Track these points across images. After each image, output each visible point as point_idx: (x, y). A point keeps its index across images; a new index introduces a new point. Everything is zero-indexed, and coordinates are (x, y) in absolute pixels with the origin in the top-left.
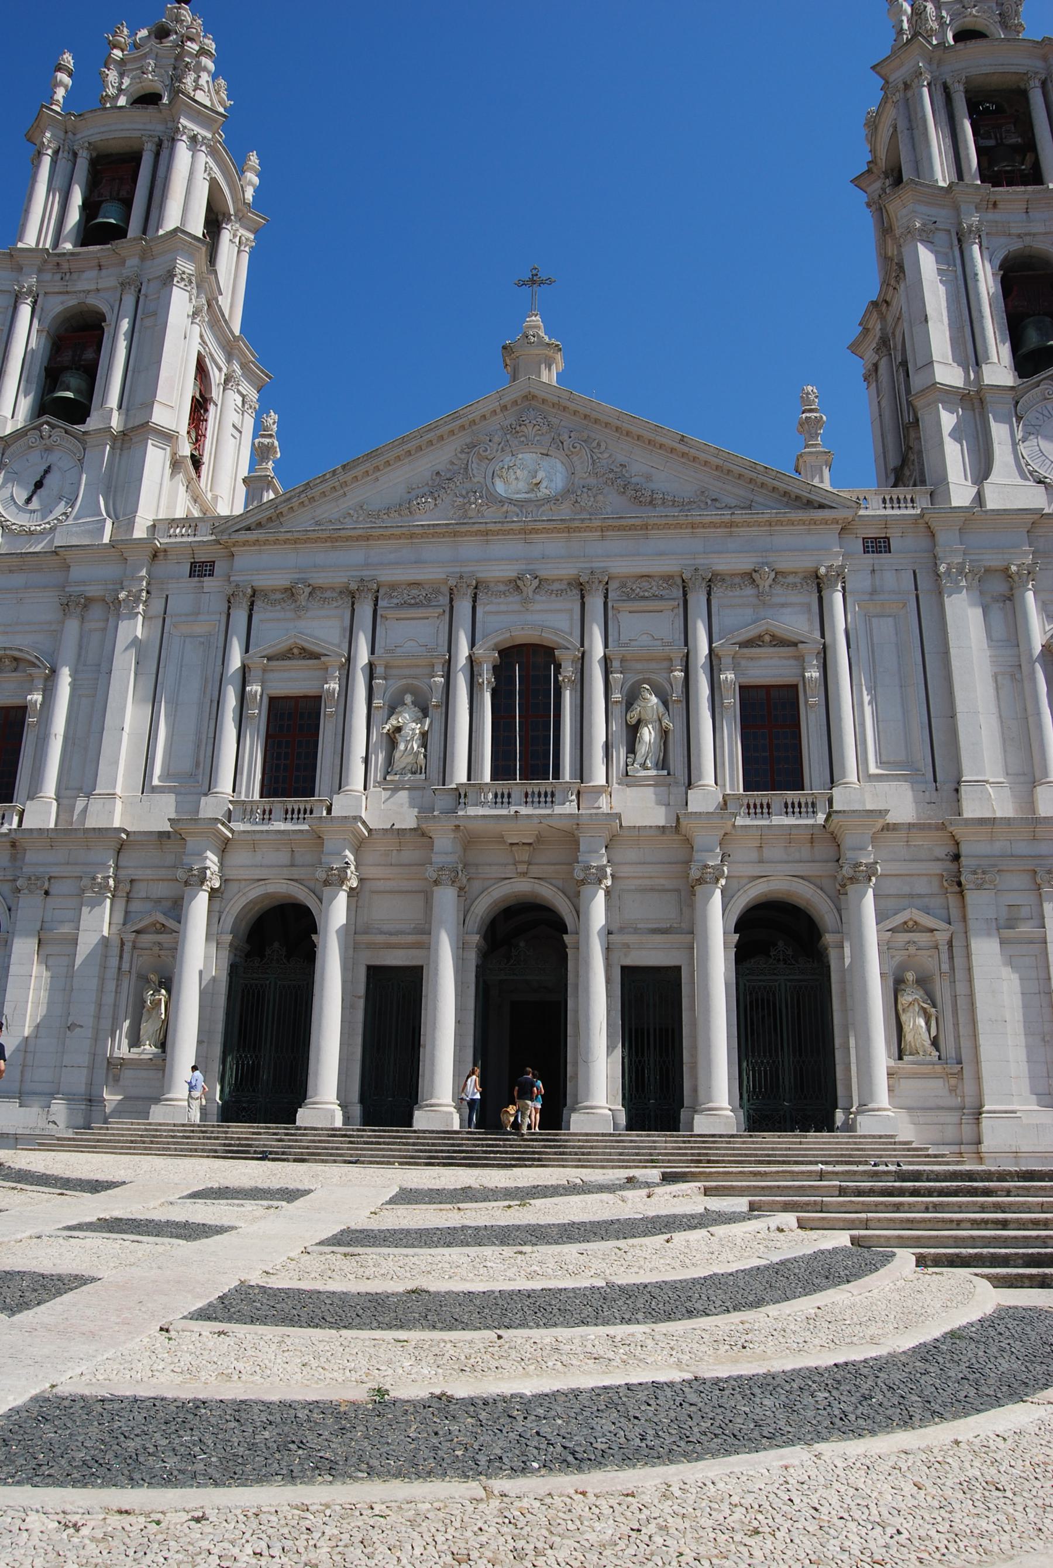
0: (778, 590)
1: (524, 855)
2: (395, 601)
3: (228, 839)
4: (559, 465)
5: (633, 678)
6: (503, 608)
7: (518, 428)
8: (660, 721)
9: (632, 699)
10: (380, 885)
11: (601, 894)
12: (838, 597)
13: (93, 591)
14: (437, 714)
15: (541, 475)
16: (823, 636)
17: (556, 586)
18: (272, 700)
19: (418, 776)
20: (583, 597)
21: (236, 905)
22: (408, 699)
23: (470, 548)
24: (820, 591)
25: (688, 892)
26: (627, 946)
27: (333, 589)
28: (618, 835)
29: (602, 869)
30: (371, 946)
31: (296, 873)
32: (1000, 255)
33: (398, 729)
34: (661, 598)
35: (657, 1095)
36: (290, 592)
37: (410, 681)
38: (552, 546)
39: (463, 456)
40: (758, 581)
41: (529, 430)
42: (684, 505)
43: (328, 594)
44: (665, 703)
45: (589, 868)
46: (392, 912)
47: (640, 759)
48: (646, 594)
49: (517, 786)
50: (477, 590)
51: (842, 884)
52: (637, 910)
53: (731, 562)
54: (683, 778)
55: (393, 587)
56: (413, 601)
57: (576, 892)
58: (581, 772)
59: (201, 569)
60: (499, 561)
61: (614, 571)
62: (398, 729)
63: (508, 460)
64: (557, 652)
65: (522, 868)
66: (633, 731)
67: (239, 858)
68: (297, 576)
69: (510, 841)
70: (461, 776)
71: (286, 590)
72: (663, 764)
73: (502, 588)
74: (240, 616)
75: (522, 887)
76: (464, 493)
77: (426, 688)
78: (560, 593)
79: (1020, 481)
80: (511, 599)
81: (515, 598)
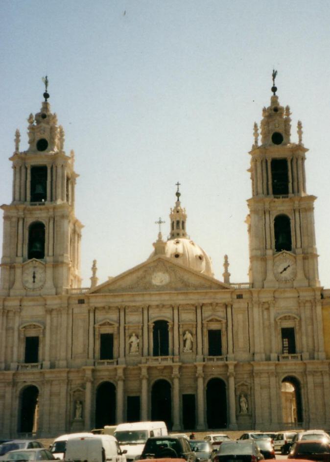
0: (217, 308)
4: (168, 277)
9: (184, 334)
13: (55, 307)
15: (163, 279)
22: (134, 335)
25: (196, 379)
33: (132, 342)
38: (166, 297)
42: (196, 288)
44: (192, 334)
46: (133, 385)
47: (186, 349)
53: (206, 301)
54: (195, 353)
55: (129, 307)
59: (81, 302)
60: (155, 300)
62: (132, 342)
66: (185, 341)
72: (191, 349)
74: (92, 315)
78: (168, 308)
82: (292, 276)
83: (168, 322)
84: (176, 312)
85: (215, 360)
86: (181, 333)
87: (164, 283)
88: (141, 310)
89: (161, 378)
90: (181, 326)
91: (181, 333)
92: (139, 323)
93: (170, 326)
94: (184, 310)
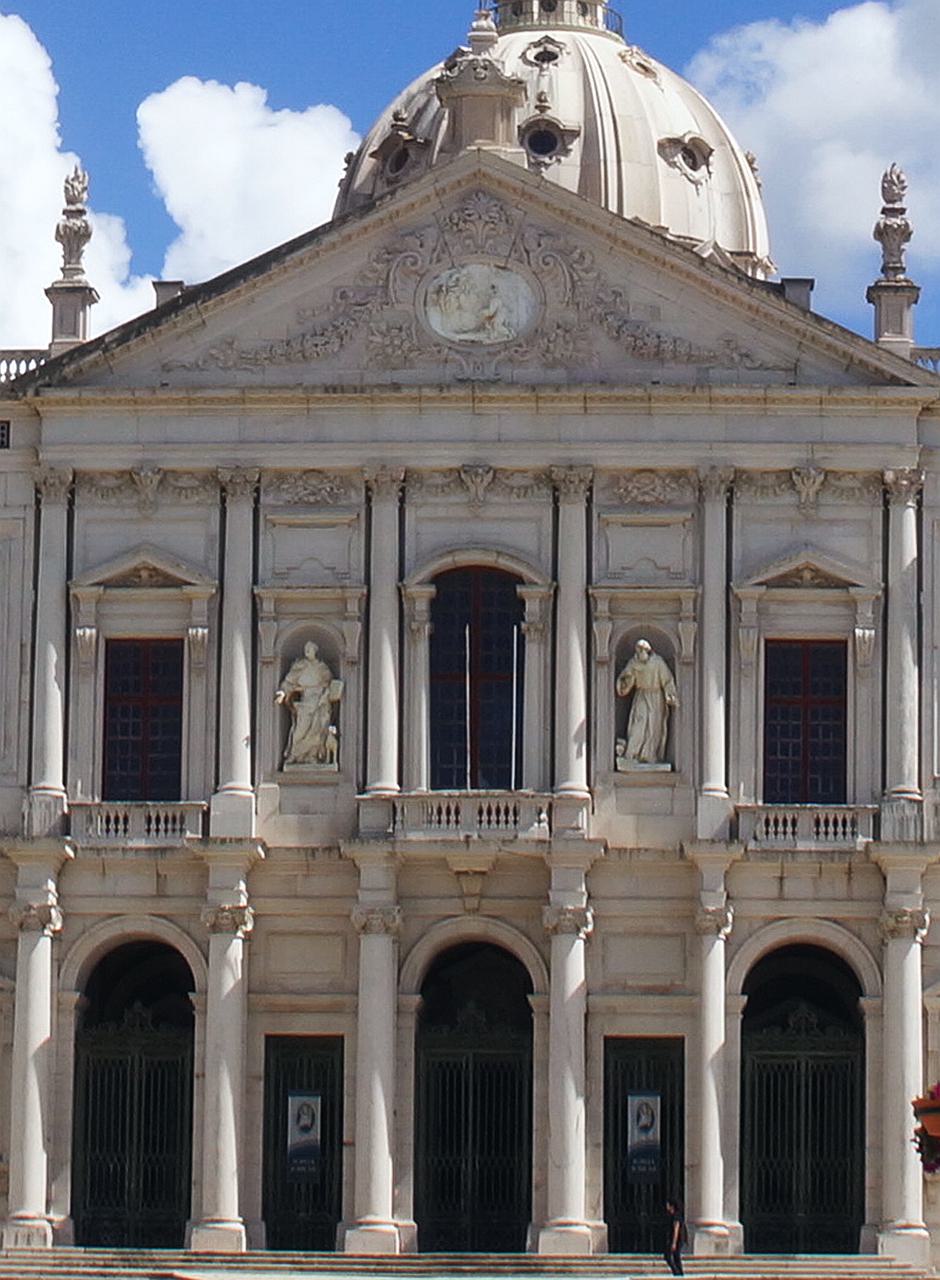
1: (476, 886)
3: (68, 859)
5: (625, 626)
6: (441, 512)
7: (461, 224)
9: (625, 653)
10: (282, 924)
11: (579, 945)
12: (910, 515)
14: (351, 675)
17: (517, 481)
18: (108, 642)
19: (328, 767)
20: (556, 501)
21: (84, 950)
22: (311, 650)
23: (395, 418)
24: (886, 503)
26: (612, 1011)
27: (191, 474)
29: (580, 915)
30: (273, 1010)
31: (165, 906)
33: (297, 696)
34: (669, 506)
36: (129, 479)
39: (379, 267)
40: (799, 486)
41: (478, 229)
43: (184, 482)
45: (562, 912)
46: (304, 963)
47: (633, 749)
48: (647, 499)
49: (469, 797)
50: (407, 485)
51: (889, 930)
52: (627, 960)
55: (281, 476)
56: (312, 499)
57: (545, 943)
58: (552, 778)
60: (435, 436)
61: (600, 464)
65: (473, 903)
66: (625, 705)
67: (85, 882)
68: (139, 456)
69: (456, 869)
70: (388, 782)
71: (123, 473)
73: (439, 480)
74: (54, 517)
75: (472, 927)
76: (384, 328)
77: (333, 632)
80: (453, 499)
81: (458, 497)
83: (520, 580)
84: (573, 515)
85: (805, 823)
86: (603, 650)
87: (499, 333)
88: (357, 497)
90: (602, 607)
91: (603, 650)
92: (340, 577)
93: (532, 607)
94: (621, 506)
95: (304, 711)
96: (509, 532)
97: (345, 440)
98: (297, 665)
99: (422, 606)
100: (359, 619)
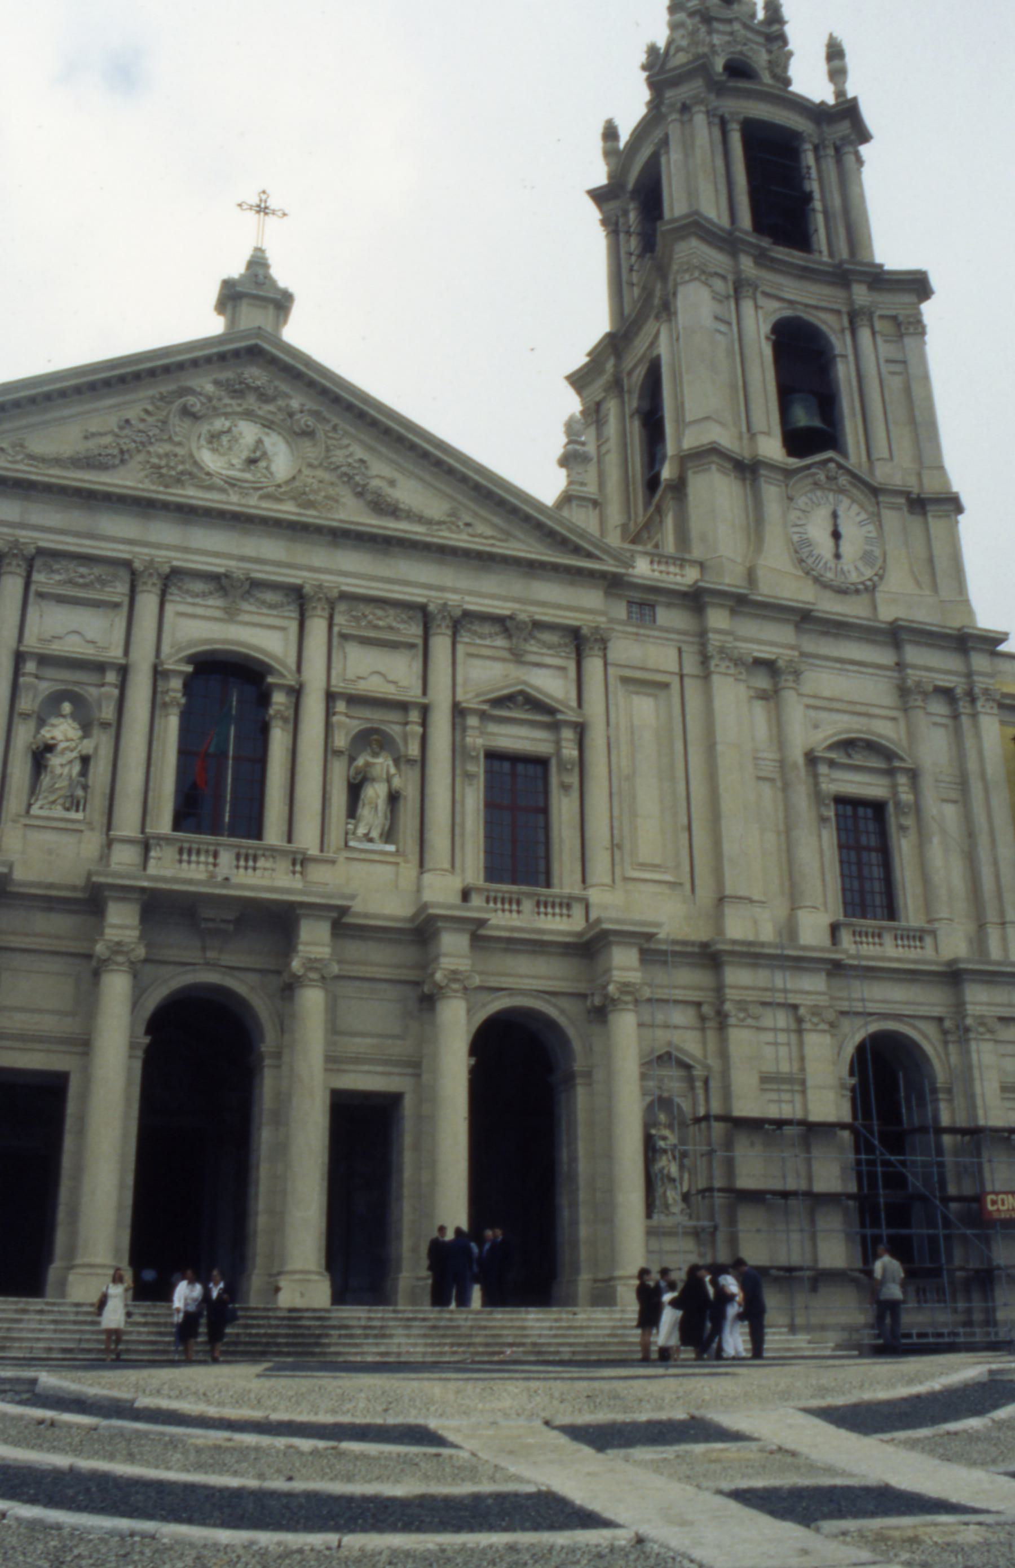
0: (532, 647)
2: (57, 577)
5: (356, 726)
8: (389, 780)
16: (580, 705)
22: (67, 707)
25: (428, 1001)
28: (343, 924)
32: (774, 318)
33: (49, 748)
35: (358, 1256)
37: (70, 687)
44: (397, 762)
47: (361, 831)
48: (381, 623)
56: (81, 581)
62: (49, 748)
63: (220, 424)
64: (270, 680)
66: (355, 791)
72: (389, 835)
79: (791, 570)
80: (211, 602)
82: (869, 573)
84: (317, 627)
86: (341, 741)
89: (212, 977)
93: (279, 699)
95: (55, 761)
96: (261, 635)
97: (118, 534)
98: (54, 721)
99: (176, 684)
100: (116, 686)
